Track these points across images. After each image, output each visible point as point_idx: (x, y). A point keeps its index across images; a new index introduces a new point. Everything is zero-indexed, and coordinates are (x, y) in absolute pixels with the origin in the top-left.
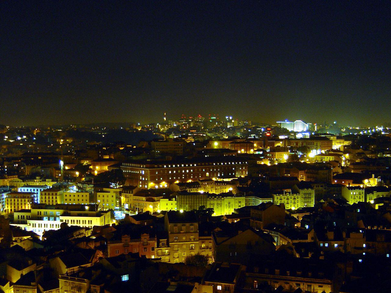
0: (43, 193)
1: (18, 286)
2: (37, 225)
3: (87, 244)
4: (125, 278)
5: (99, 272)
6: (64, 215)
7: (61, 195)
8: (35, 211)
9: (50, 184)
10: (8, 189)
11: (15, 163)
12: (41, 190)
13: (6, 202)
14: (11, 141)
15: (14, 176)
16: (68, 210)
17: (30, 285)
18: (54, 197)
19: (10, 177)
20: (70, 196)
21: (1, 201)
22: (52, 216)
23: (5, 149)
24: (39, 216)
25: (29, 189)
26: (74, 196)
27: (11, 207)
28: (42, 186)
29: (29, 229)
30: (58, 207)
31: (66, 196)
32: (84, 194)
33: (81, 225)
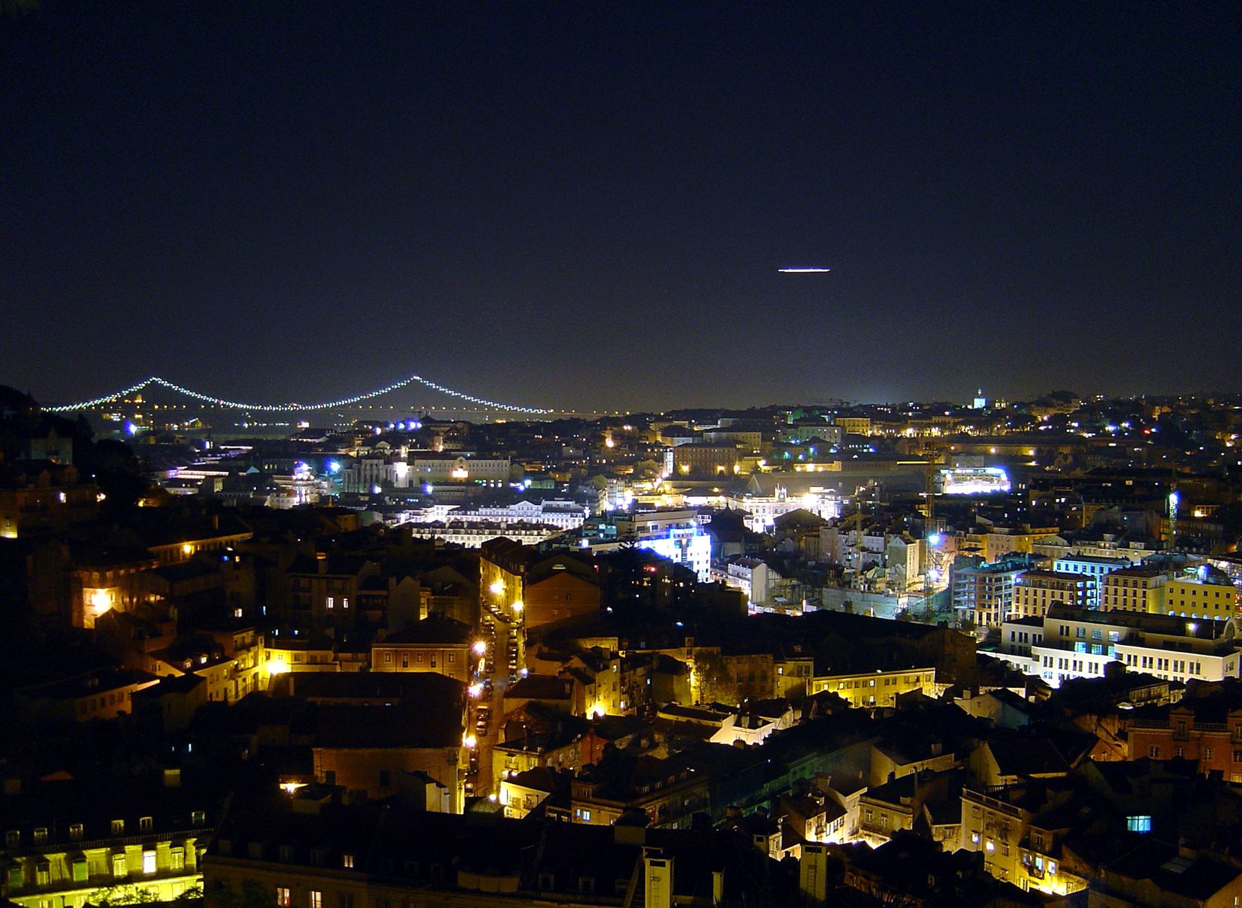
0: (1112, 579)
1: (869, 799)
2: (1056, 663)
3: (1099, 720)
4: (1141, 824)
5: (1064, 796)
6: (1128, 641)
7: (1159, 587)
8: (1053, 624)
9: (1137, 555)
10: (1027, 561)
11: (1060, 495)
12: (1102, 569)
13: (1014, 596)
14: (1086, 435)
15: (1050, 530)
16: (1142, 629)
17: (898, 803)
18: (1140, 592)
19: (1037, 530)
20: (1183, 592)
21: (1004, 592)
22: (1098, 641)
23: (1066, 457)
24: (1064, 637)
25: (1080, 564)
26: (1194, 593)
27: (1026, 609)
28: (1115, 561)
29: (1035, 669)
30: (1114, 618)
31: (1171, 590)
32: (1223, 590)
33: (1155, 672)
